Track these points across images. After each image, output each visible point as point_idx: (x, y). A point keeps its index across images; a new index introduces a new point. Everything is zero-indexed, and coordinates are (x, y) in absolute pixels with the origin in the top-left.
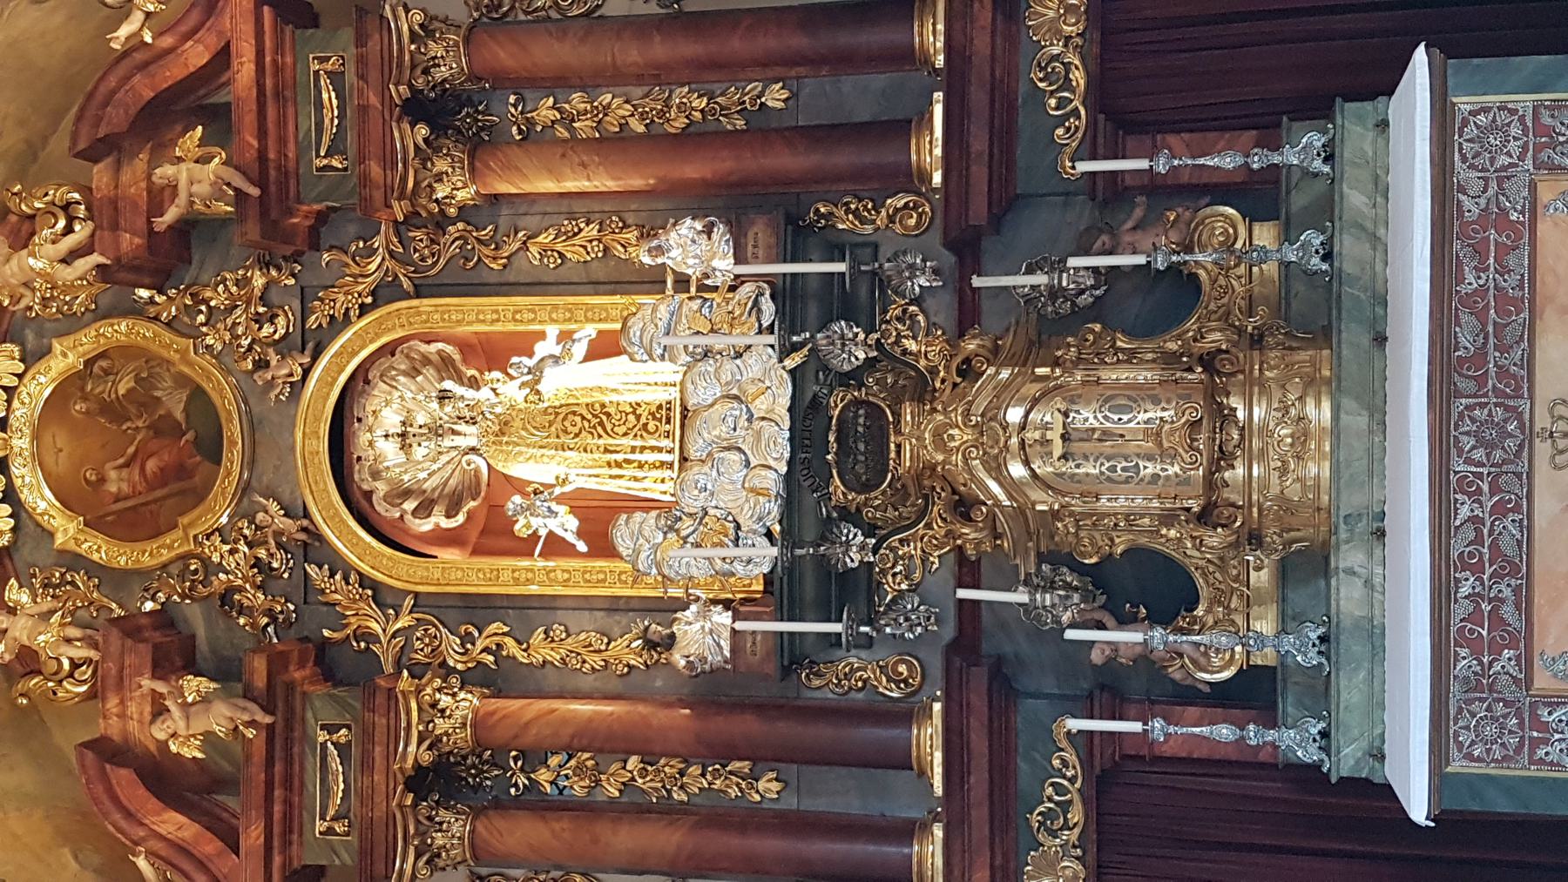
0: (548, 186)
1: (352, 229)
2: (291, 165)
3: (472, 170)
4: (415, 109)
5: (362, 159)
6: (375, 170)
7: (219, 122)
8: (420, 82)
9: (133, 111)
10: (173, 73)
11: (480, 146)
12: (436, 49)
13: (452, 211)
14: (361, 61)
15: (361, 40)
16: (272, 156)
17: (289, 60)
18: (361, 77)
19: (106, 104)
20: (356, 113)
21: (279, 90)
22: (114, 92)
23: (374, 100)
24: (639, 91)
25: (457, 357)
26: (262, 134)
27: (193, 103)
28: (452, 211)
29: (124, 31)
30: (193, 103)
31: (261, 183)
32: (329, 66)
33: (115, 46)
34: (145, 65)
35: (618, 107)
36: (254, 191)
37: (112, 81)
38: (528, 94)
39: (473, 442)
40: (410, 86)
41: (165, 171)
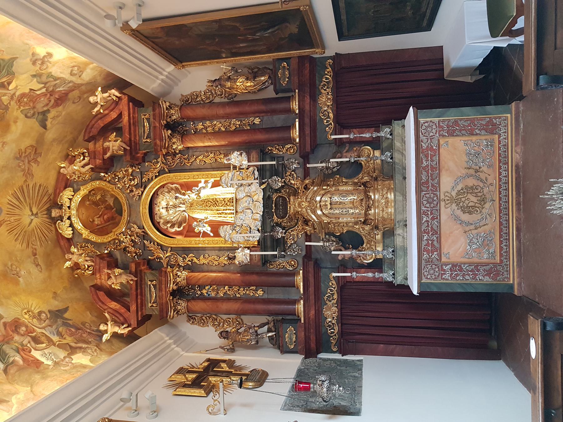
0: (202, 144)
1: (153, 157)
2: (137, 141)
3: (182, 141)
4: (168, 126)
5: (155, 139)
6: (158, 142)
7: (119, 131)
8: (169, 120)
9: (98, 130)
10: (108, 120)
11: (184, 135)
12: (172, 112)
13: (178, 152)
14: (154, 115)
15: (154, 110)
16: (133, 139)
17: (136, 115)
18: (154, 119)
19: (92, 128)
20: (153, 128)
21: (134, 123)
22: (94, 125)
23: (157, 125)
24: (223, 120)
25: (180, 188)
26: (130, 134)
27: (113, 127)
28: (178, 152)
29: (96, 110)
30: (113, 127)
31: (130, 146)
32: (146, 117)
33: (94, 113)
34: (101, 118)
35: (218, 125)
36: (128, 148)
37: (93, 122)
38: (196, 122)
39: (184, 209)
40: (166, 121)
41: (107, 144)
